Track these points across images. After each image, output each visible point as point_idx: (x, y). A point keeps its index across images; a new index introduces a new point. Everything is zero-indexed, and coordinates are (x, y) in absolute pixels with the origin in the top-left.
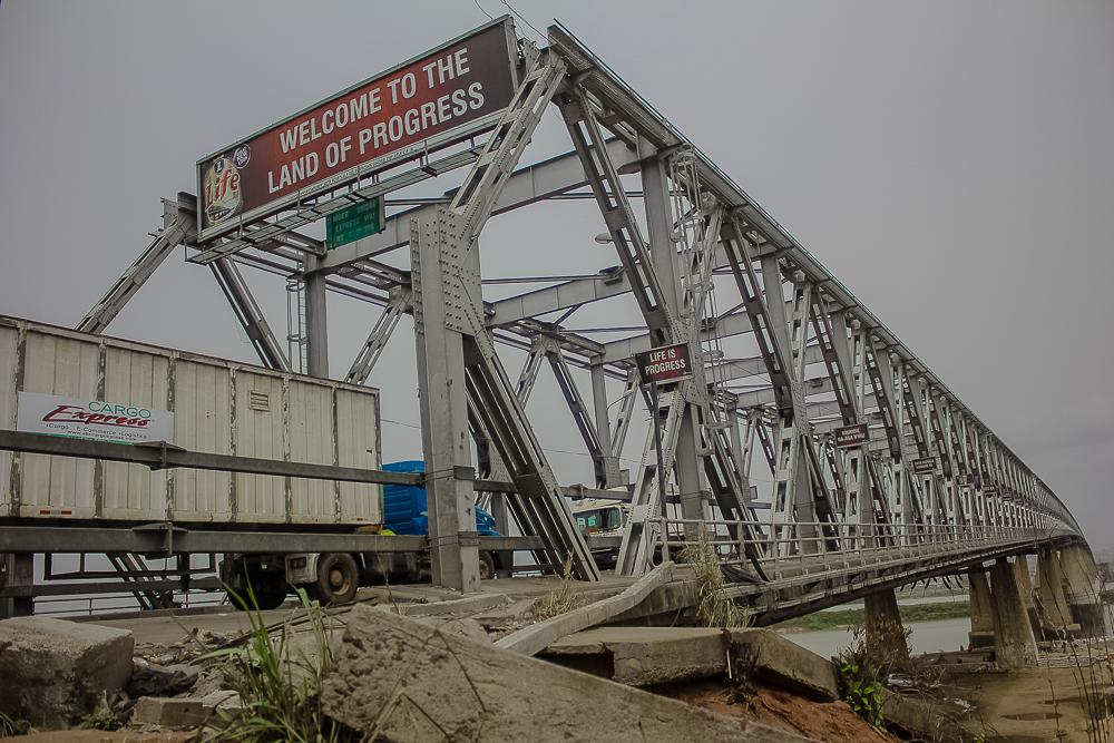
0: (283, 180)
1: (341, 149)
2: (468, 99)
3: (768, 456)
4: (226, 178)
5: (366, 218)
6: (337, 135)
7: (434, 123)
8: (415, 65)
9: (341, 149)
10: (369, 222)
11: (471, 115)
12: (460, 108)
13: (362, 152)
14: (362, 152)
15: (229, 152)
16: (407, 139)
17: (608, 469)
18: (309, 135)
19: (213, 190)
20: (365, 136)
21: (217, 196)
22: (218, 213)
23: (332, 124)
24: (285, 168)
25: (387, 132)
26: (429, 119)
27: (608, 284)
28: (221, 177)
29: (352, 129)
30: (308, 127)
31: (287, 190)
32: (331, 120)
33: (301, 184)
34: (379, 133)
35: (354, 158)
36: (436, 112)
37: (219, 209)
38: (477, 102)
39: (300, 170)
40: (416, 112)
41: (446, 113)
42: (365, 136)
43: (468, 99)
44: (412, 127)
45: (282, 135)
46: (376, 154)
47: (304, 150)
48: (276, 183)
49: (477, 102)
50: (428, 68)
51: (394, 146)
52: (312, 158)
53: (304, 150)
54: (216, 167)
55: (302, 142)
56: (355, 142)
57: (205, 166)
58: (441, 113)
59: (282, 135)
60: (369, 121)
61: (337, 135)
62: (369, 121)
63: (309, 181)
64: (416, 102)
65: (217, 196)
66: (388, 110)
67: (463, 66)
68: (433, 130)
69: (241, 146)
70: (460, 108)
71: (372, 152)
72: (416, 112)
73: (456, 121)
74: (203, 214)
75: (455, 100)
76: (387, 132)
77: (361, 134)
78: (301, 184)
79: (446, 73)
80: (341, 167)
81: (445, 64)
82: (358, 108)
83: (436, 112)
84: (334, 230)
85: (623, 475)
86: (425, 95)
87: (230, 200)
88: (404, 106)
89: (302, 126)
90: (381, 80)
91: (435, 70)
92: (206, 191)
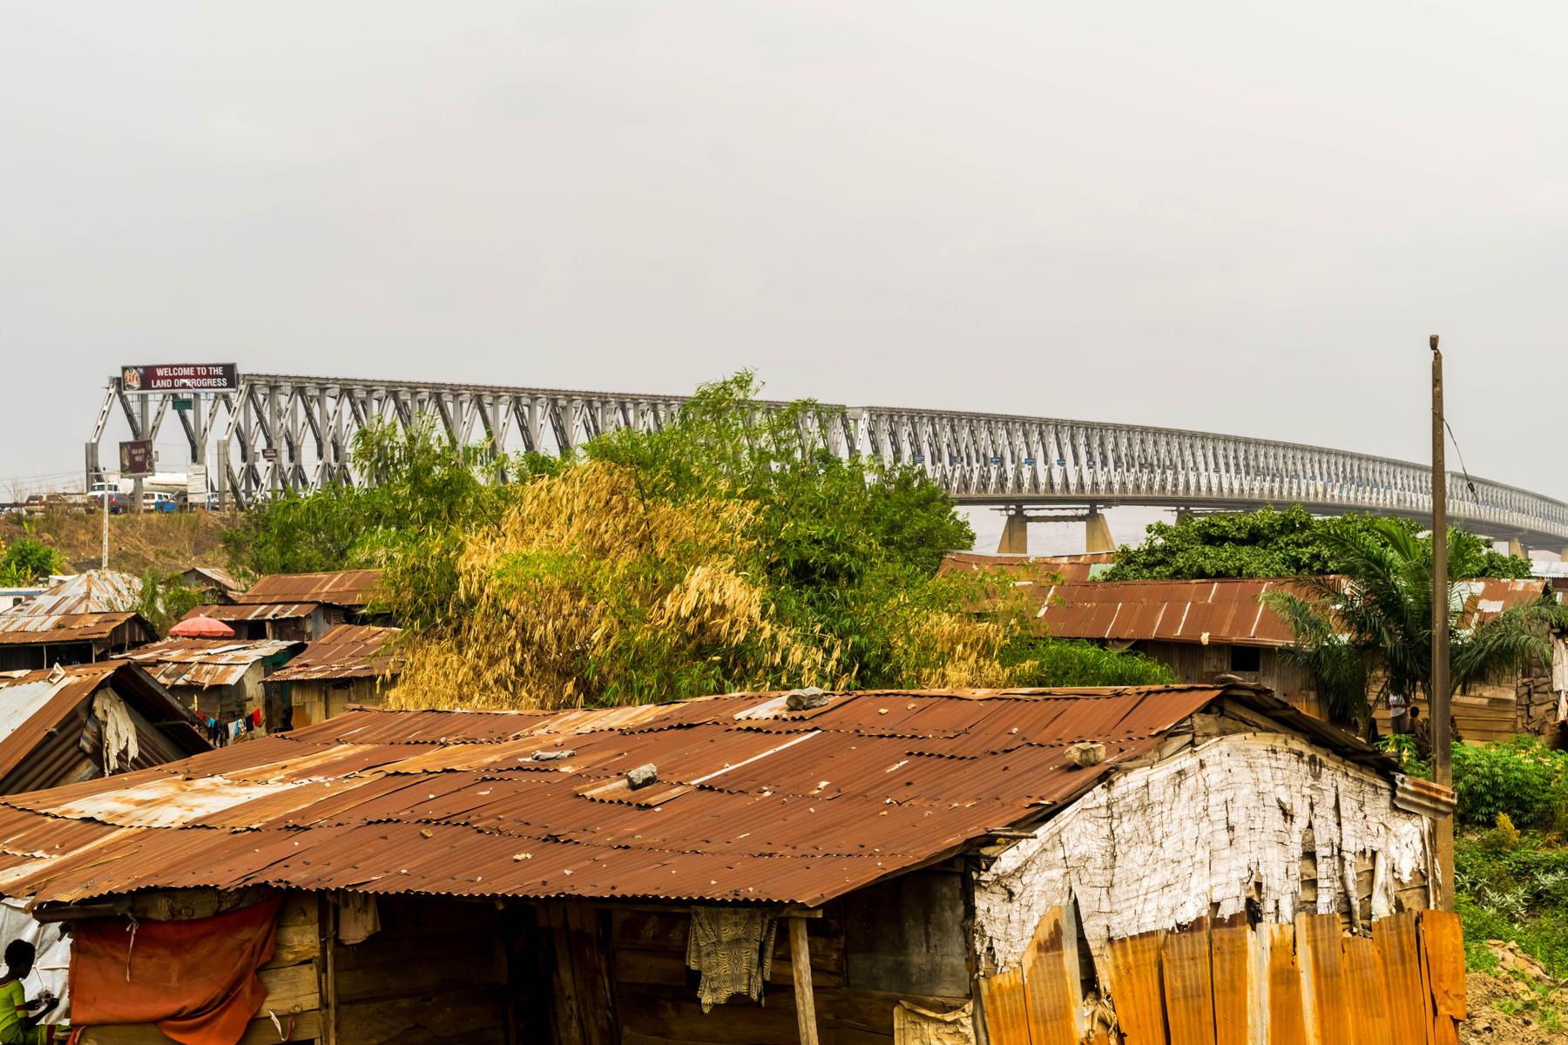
8: (207, 366)
11: (222, 387)
15: (136, 368)
17: (249, 452)
31: (159, 388)
33: (164, 388)
57: (124, 369)
61: (179, 377)
63: (167, 388)
66: (196, 376)
68: (210, 387)
73: (217, 387)
78: (164, 388)
86: (208, 376)
87: (136, 384)
88: (201, 377)
90: (195, 366)
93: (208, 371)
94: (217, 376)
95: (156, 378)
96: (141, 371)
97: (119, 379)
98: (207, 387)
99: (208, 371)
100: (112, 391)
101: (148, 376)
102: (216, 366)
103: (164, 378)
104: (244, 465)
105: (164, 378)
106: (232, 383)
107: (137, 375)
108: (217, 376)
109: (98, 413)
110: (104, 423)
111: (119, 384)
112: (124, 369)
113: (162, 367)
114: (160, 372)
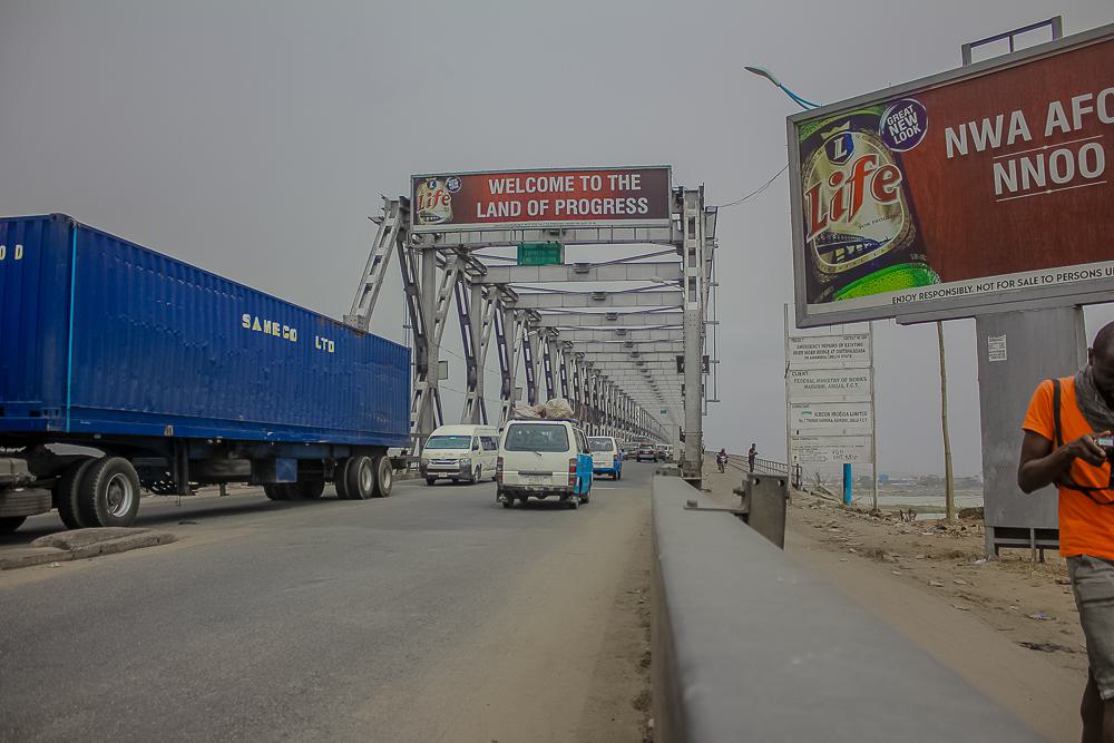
0: (489, 211)
1: (542, 206)
2: (637, 205)
3: (467, 351)
4: (438, 195)
5: (550, 252)
6: (538, 196)
7: (612, 212)
8: (604, 173)
9: (542, 206)
10: (552, 256)
11: (637, 216)
12: (631, 209)
13: (557, 213)
14: (557, 213)
15: (442, 178)
16: (591, 216)
18: (514, 188)
19: (425, 199)
20: (560, 204)
21: (429, 205)
22: (435, 219)
23: (534, 188)
24: (492, 204)
25: (577, 207)
26: (609, 209)
27: (578, 273)
28: (434, 192)
29: (552, 196)
30: (514, 182)
31: (492, 219)
32: (532, 185)
33: (504, 219)
34: (571, 205)
35: (549, 215)
36: (615, 206)
37: (430, 215)
38: (643, 209)
39: (504, 209)
40: (600, 202)
41: (621, 209)
42: (560, 204)
43: (637, 205)
44: (597, 210)
45: (490, 181)
46: (567, 218)
47: (511, 197)
48: (484, 211)
49: (643, 209)
50: (613, 177)
51: (579, 217)
52: (516, 205)
53: (511, 197)
54: (428, 185)
55: (508, 191)
56: (552, 205)
57: (418, 182)
58: (618, 209)
59: (490, 181)
60: (566, 196)
61: (538, 196)
62: (566, 196)
63: (510, 219)
64: (602, 195)
65: (429, 205)
66: (578, 194)
67: (637, 185)
68: (609, 216)
69: (454, 177)
70: (631, 209)
71: (563, 215)
72: (600, 202)
74: (416, 215)
75: (628, 203)
76: (577, 207)
77: (557, 201)
79: (624, 185)
80: (538, 218)
81: (624, 179)
82: (555, 184)
83: (615, 206)
84: (523, 254)
85: (518, 391)
86: (606, 192)
87: (443, 212)
88: (591, 195)
89: (508, 181)
90: (576, 173)
91: (616, 180)
92: (418, 199)
93: (606, 183)
94: (626, 194)
95: (487, 198)
96: (454, 184)
97: (406, 202)
98: (602, 217)
99: (606, 183)
100: (393, 222)
101: (469, 195)
102: (624, 172)
103: (505, 197)
104: (507, 403)
105: (505, 197)
106: (658, 210)
107: (446, 192)
108: (626, 194)
109: (363, 259)
110: (380, 281)
111: (405, 212)
112: (418, 182)
113: (500, 175)
114: (495, 187)
